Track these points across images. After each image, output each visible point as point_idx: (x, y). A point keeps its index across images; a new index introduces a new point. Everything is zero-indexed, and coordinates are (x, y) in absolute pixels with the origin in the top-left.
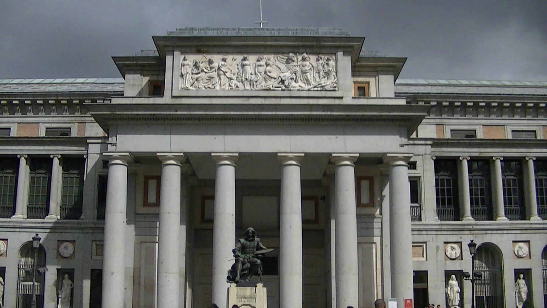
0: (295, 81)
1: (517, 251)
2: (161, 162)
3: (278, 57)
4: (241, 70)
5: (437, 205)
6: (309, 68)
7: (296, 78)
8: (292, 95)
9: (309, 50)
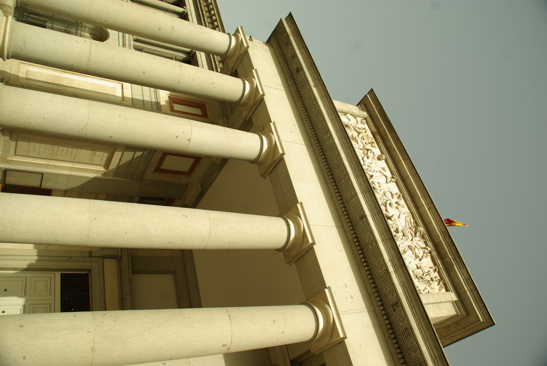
3: (409, 217)
6: (417, 254)
9: (434, 253)
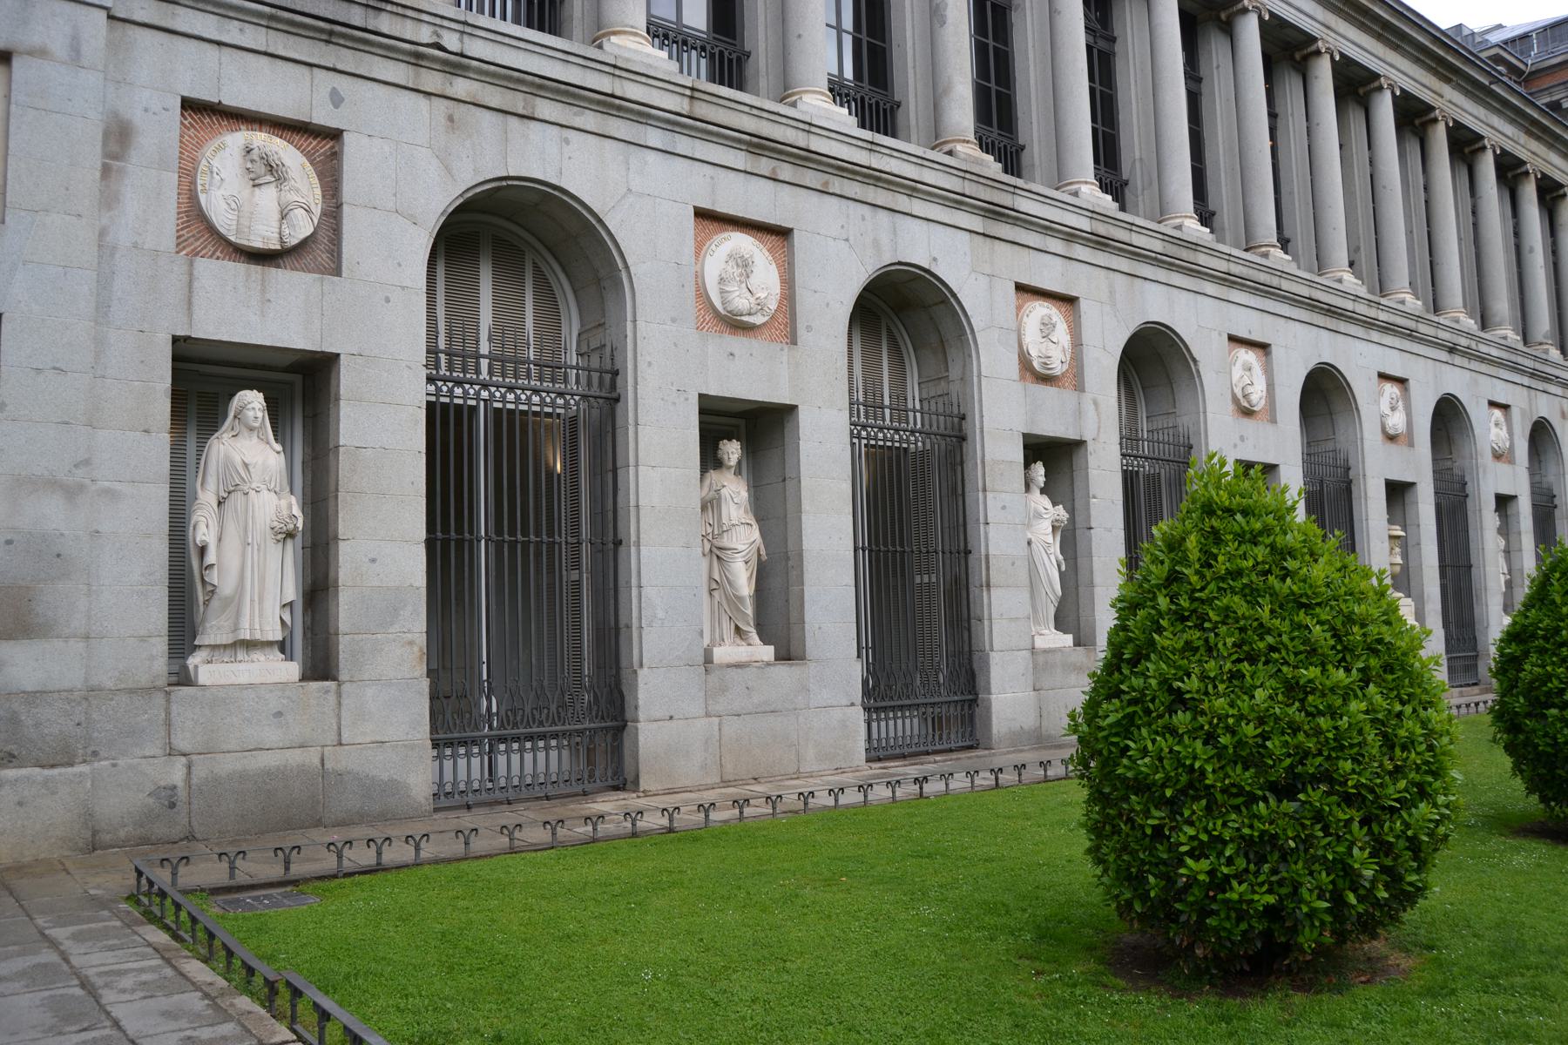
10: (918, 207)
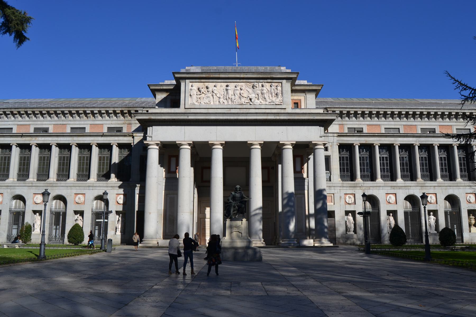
0: (258, 99)
1: (389, 200)
2: (179, 147)
4: (226, 92)
5: (340, 172)
7: (258, 98)
8: (256, 108)
9: (265, 81)
10: (412, 188)
